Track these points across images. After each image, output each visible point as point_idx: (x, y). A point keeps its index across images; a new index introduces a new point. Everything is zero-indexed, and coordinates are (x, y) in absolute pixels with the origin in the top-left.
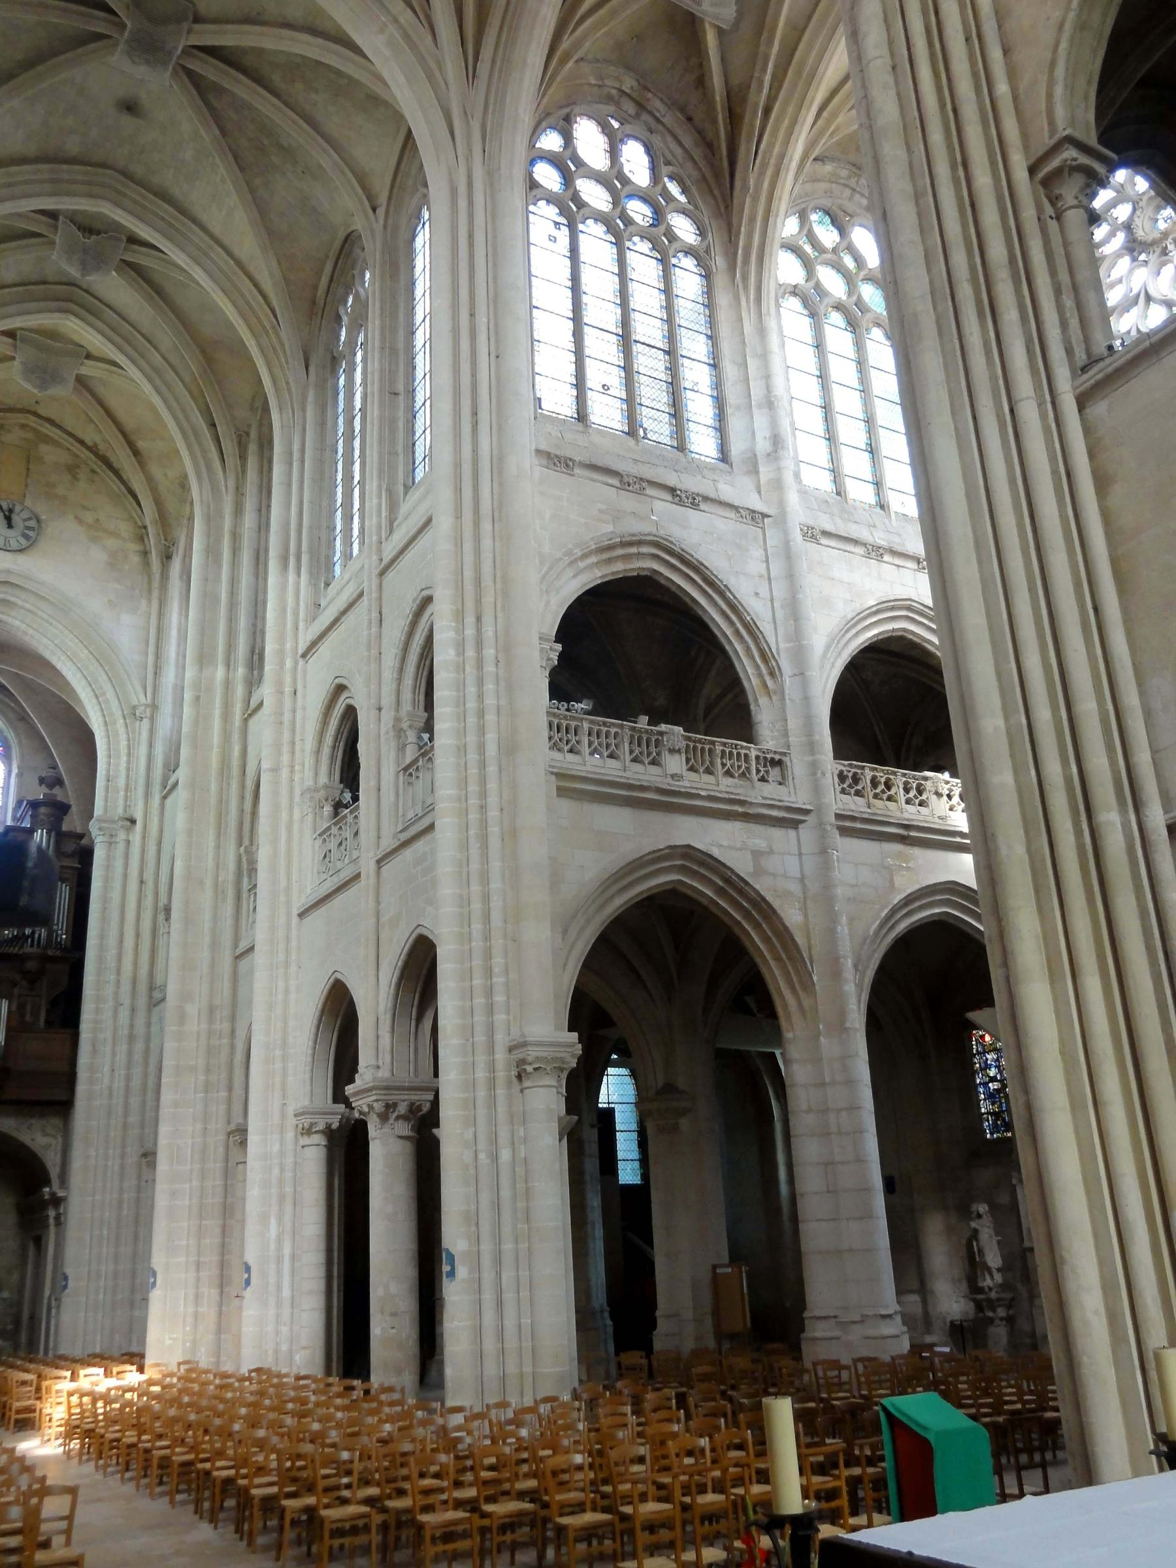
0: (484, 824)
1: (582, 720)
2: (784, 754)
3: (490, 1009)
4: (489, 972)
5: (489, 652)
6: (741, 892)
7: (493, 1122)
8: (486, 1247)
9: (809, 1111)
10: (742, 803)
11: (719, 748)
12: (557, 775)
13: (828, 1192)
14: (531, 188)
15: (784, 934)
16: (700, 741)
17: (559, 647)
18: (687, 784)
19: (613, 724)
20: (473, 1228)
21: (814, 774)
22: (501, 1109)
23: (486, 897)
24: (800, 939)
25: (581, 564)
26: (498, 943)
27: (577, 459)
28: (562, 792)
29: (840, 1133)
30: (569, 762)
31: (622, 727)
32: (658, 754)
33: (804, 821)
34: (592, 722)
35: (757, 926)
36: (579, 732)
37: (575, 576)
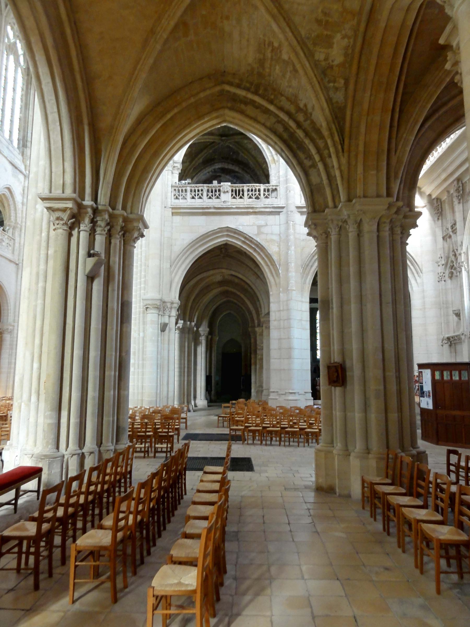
1: (187, 186)
2: (277, 186)
6: (251, 241)
9: (275, 320)
10: (252, 208)
11: (246, 189)
12: (173, 208)
13: (279, 349)
15: (269, 256)
16: (237, 187)
18: (229, 204)
19: (200, 186)
21: (287, 192)
24: (275, 258)
29: (284, 328)
30: (181, 203)
31: (203, 186)
32: (220, 195)
33: (282, 212)
34: (191, 187)
35: (259, 254)
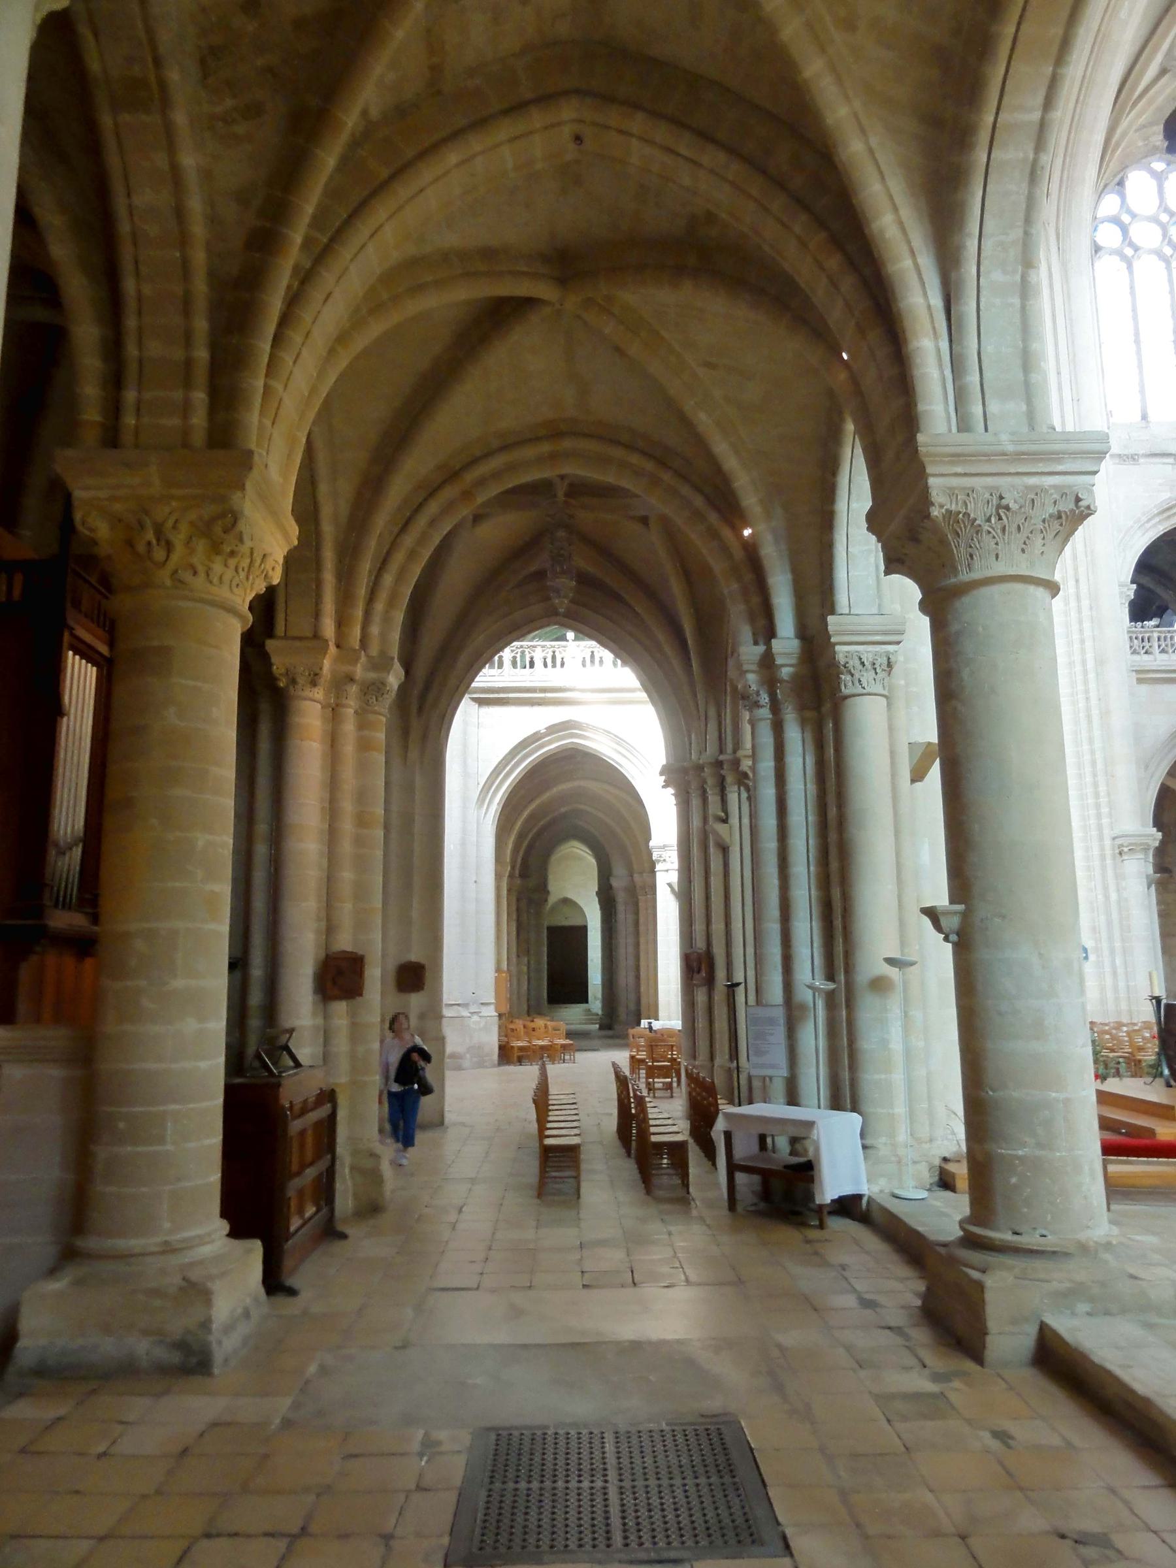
0: (1088, 709)
3: (1099, 816)
4: (1097, 795)
5: (1085, 603)
7: (1104, 876)
8: (1105, 945)
14: (1096, 252)
17: (1134, 586)
20: (1098, 935)
22: (1110, 872)
23: (1093, 752)
25: (1148, 525)
26: (1101, 779)
27: (1141, 452)
28: (1140, 681)
30: (1144, 660)
36: (1151, 640)
37: (1144, 534)
